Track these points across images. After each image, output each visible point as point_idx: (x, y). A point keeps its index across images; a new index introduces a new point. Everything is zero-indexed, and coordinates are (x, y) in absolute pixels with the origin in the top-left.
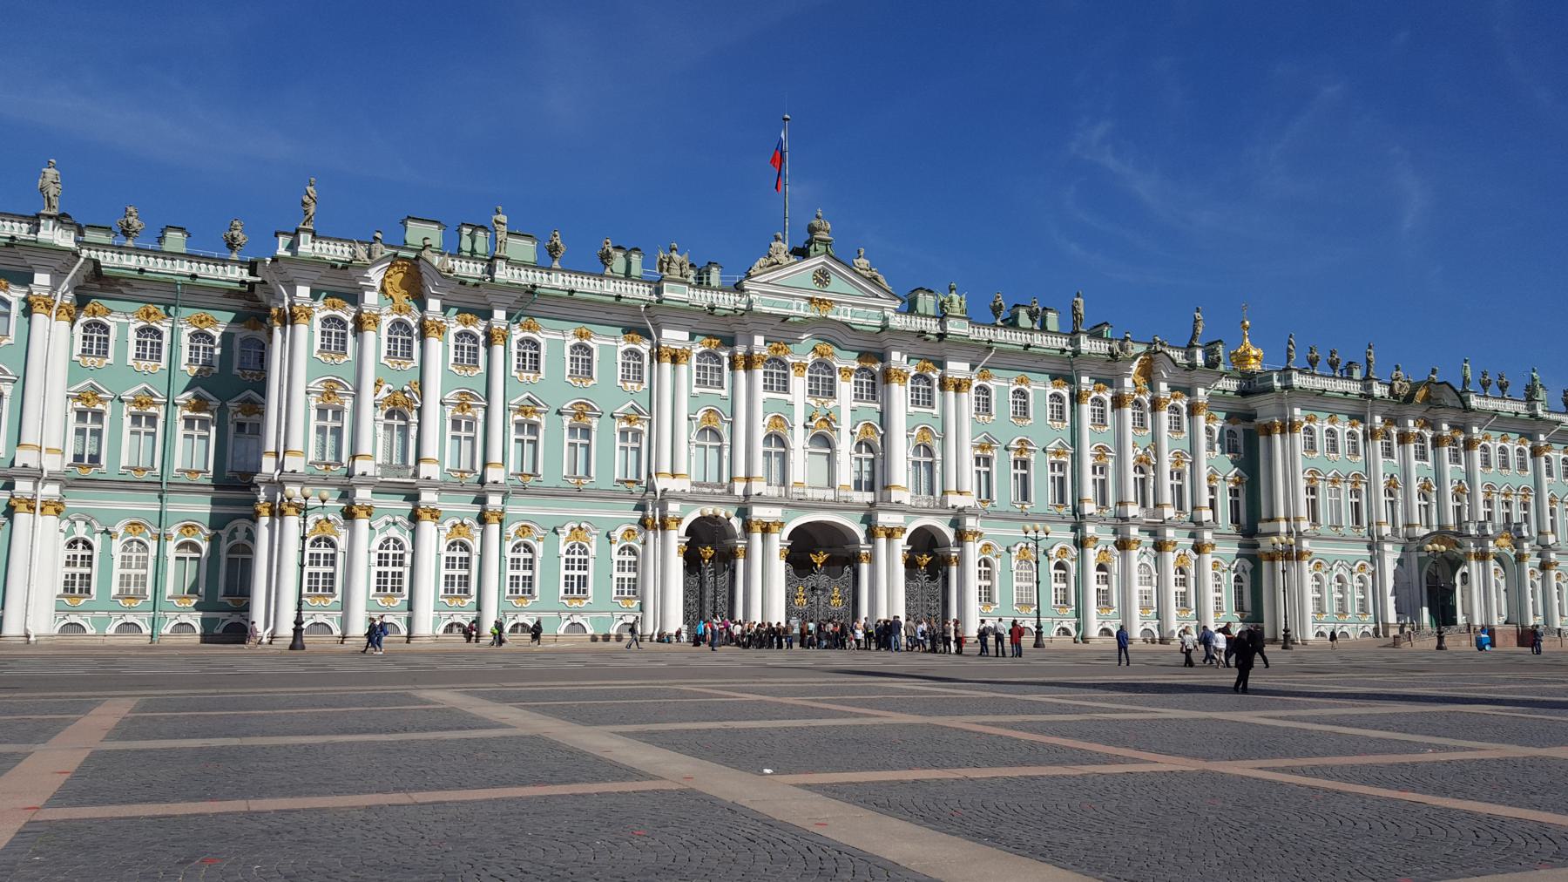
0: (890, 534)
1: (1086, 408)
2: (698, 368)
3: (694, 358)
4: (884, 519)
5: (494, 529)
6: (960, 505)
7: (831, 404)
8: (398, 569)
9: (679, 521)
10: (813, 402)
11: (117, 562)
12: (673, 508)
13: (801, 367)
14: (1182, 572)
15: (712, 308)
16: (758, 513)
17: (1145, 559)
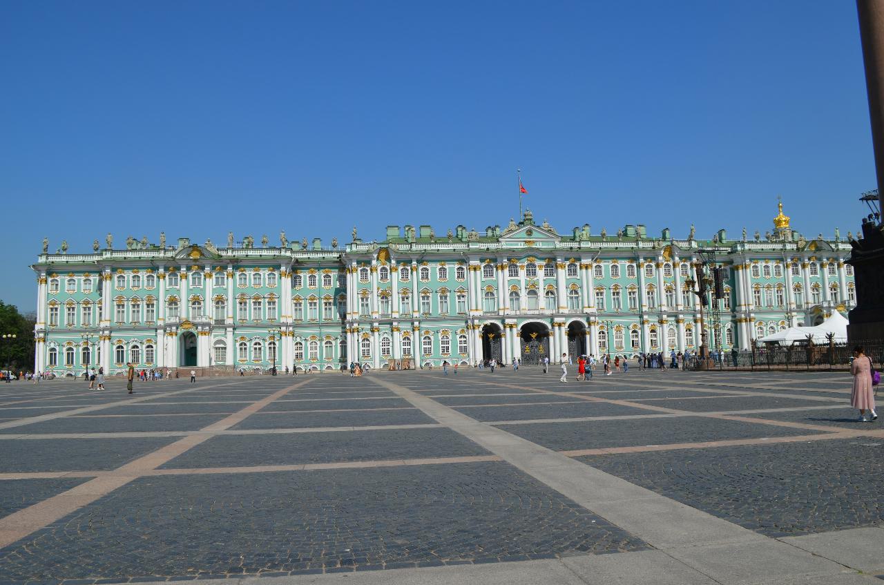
0: (560, 325)
1: (643, 271)
2: (484, 271)
3: (482, 269)
4: (557, 320)
5: (417, 332)
6: (588, 312)
7: (536, 279)
8: (388, 347)
9: (479, 326)
10: (528, 279)
11: (309, 348)
12: (476, 322)
13: (522, 267)
14: (690, 330)
15: (488, 249)
16: (508, 321)
17: (672, 327)
